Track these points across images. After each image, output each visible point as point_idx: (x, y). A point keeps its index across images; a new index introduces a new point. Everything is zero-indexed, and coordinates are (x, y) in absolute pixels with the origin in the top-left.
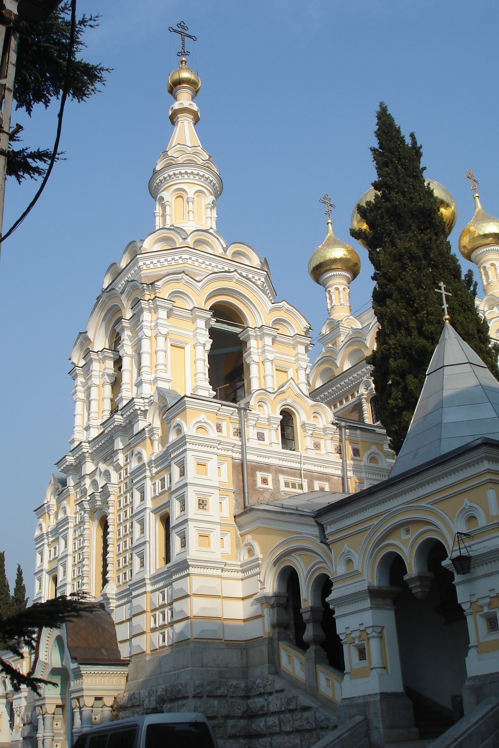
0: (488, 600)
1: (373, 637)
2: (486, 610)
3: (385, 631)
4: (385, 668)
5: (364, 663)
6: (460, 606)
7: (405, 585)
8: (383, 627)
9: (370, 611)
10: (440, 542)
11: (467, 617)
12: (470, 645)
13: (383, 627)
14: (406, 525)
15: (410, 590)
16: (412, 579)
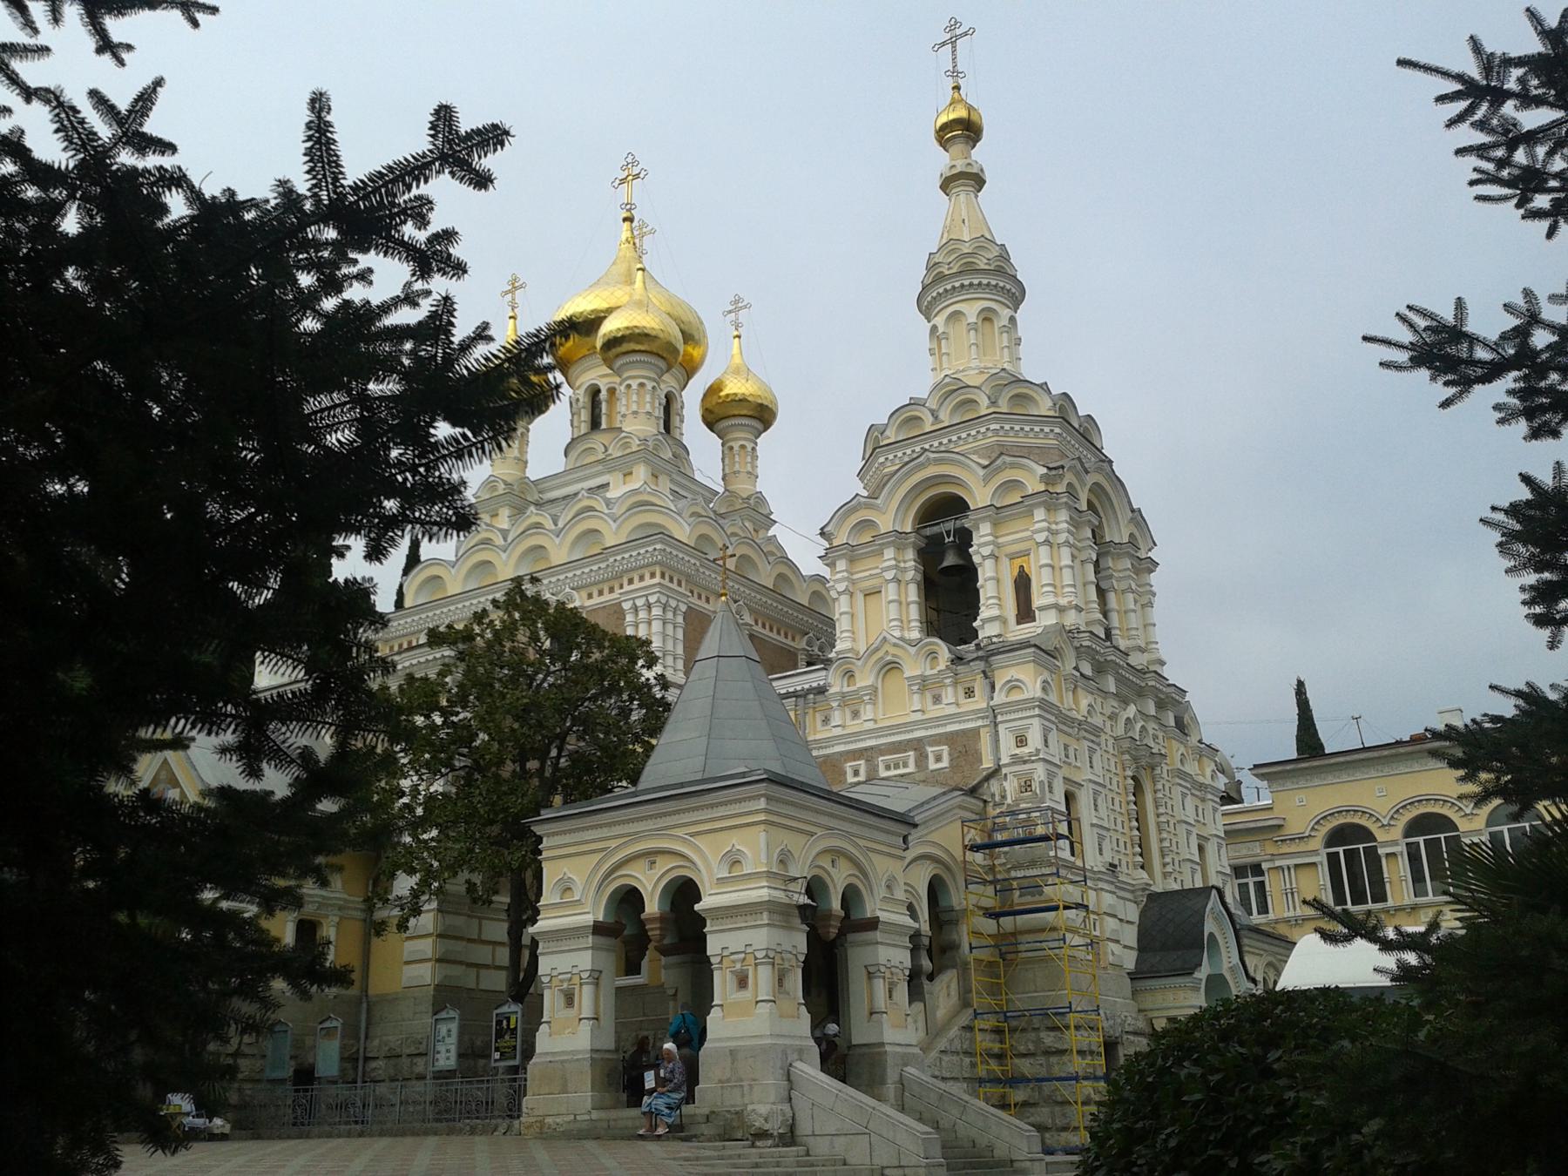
0: (743, 955)
1: (587, 983)
2: (738, 966)
3: (603, 975)
4: (597, 1019)
5: (572, 1012)
6: (708, 958)
7: (642, 924)
8: (601, 972)
9: (590, 952)
10: (691, 879)
11: (715, 973)
12: (714, 1003)
13: (601, 972)
14: (651, 855)
15: (646, 931)
16: (652, 920)
